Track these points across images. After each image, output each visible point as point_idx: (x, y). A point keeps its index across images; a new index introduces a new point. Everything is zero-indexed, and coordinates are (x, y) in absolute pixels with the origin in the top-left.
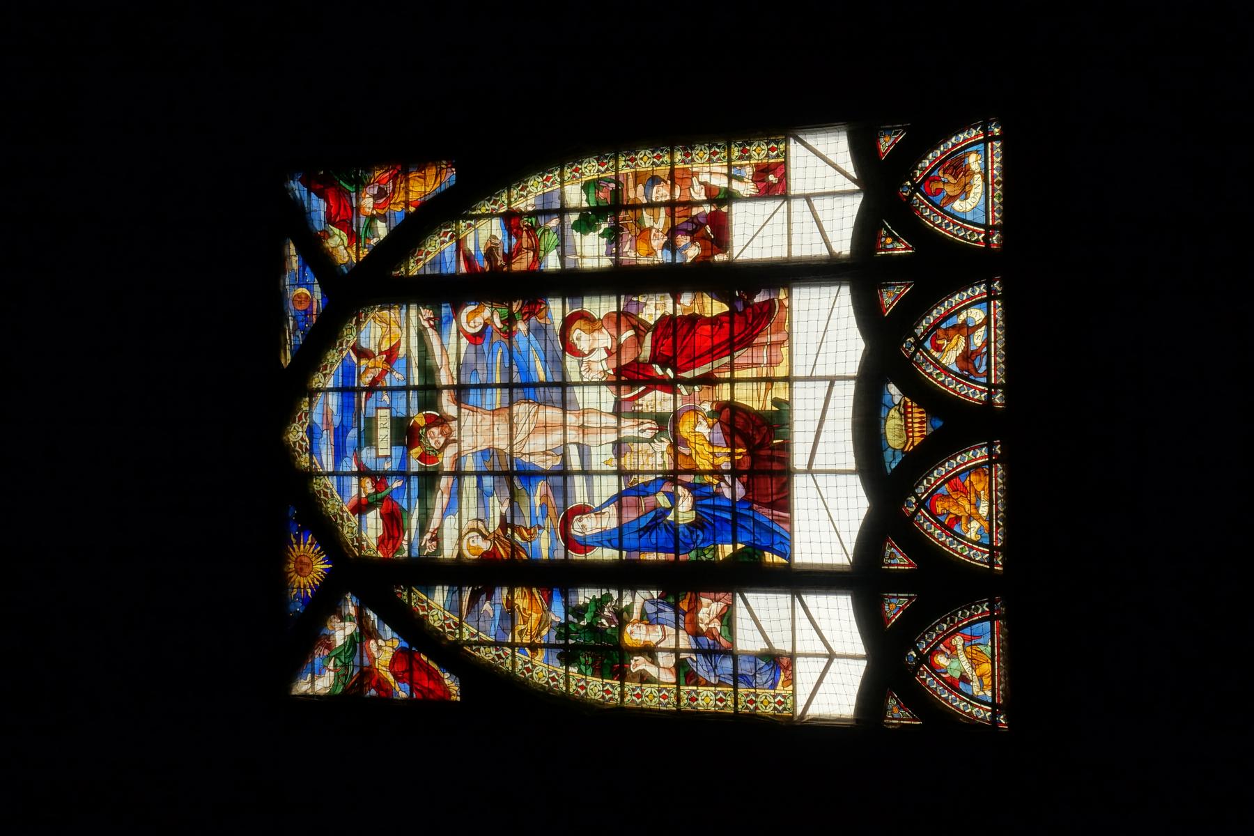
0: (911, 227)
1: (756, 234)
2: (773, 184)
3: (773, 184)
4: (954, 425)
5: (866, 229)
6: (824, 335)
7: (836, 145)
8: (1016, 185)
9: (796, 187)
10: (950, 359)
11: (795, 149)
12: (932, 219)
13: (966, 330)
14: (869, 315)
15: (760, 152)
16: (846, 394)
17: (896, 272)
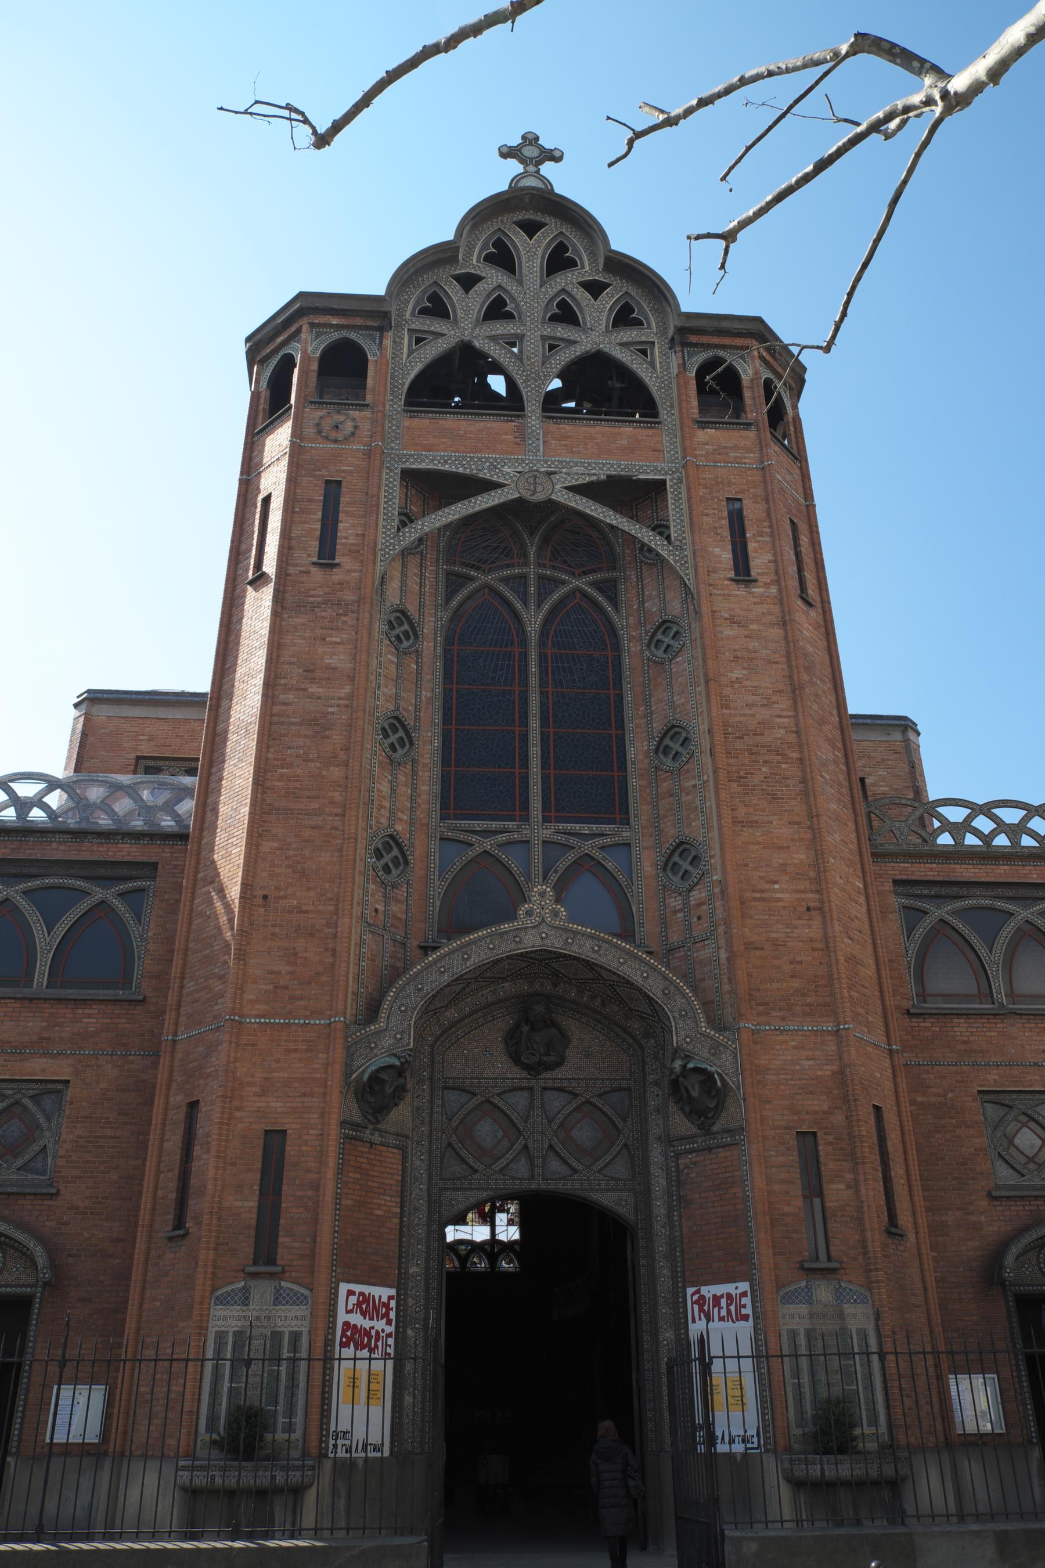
0: (500, 1252)
1: (501, 1218)
2: (510, 1223)
3: (510, 1223)
4: (463, 1260)
5: (501, 1242)
6: (480, 1233)
7: (517, 1236)
8: (507, 1274)
9: (510, 1228)
10: (475, 1260)
11: (516, 1228)
12: (502, 1256)
13: (480, 1263)
14: (484, 1243)
15: (517, 1220)
16: (469, 1237)
17: (493, 1248)
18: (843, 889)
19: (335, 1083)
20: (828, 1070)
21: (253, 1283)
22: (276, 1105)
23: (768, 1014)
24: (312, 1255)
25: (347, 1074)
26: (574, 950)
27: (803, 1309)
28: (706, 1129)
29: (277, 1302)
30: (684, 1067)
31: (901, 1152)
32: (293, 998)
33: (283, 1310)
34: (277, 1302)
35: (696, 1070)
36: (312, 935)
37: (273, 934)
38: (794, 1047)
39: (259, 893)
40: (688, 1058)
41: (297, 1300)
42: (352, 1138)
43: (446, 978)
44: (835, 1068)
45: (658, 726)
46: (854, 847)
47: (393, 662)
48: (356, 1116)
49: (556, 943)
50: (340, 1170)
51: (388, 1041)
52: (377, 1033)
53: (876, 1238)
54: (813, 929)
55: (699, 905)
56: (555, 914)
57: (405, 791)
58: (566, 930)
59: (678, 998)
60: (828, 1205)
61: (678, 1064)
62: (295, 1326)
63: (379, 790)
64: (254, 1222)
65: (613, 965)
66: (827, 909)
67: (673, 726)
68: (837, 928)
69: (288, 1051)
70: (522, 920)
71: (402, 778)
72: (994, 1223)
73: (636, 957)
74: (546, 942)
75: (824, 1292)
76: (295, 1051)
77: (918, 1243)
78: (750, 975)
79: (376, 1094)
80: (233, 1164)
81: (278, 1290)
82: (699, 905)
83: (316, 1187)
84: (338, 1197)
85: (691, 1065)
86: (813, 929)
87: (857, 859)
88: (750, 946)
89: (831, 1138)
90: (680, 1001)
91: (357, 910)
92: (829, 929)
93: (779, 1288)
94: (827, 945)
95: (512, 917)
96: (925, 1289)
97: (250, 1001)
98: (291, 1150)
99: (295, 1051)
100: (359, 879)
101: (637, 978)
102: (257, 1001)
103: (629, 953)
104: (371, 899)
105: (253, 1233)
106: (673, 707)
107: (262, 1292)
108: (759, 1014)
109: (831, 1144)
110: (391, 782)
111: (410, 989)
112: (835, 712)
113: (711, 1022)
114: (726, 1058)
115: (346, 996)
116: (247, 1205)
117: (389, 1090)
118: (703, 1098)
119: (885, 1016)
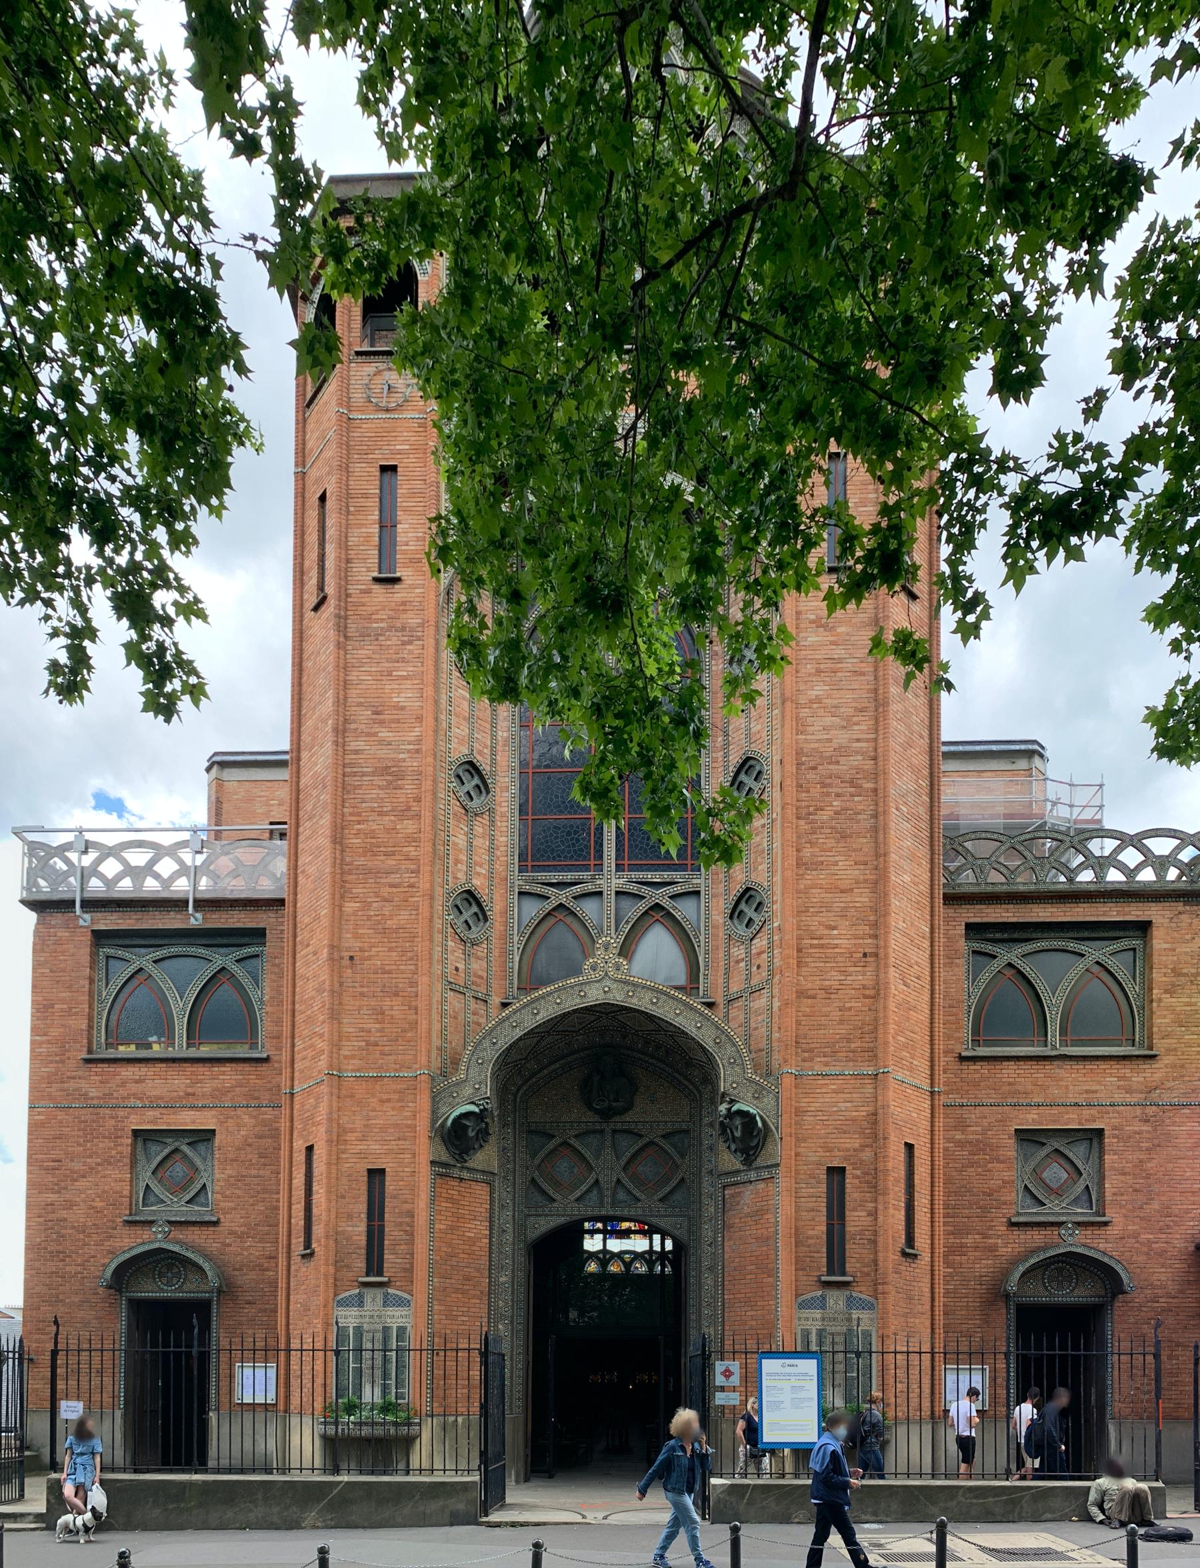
18: (906, 935)
19: (423, 1125)
20: (863, 1112)
21: (365, 1290)
22: (375, 1147)
23: (811, 1060)
24: (411, 1270)
25: (433, 1122)
26: (634, 1003)
27: (817, 1314)
28: (749, 1161)
29: (385, 1304)
30: (729, 1110)
31: (928, 1184)
32: (382, 1054)
33: (390, 1311)
34: (385, 1304)
35: (740, 1113)
36: (396, 994)
37: (362, 994)
38: (834, 1091)
39: (346, 954)
40: (732, 1101)
41: (401, 1303)
42: (441, 1175)
43: (519, 1033)
44: (871, 1109)
45: (735, 759)
46: (925, 888)
47: (464, 698)
48: (445, 1157)
49: (617, 997)
50: (433, 1200)
51: (468, 1091)
52: (457, 1084)
53: (890, 1256)
54: (861, 977)
55: (759, 954)
56: (618, 967)
57: (481, 843)
58: (626, 982)
59: (728, 1046)
60: (848, 1229)
61: (723, 1108)
62: (401, 1322)
63: (456, 844)
64: (364, 1243)
65: (669, 1017)
66: (881, 955)
67: (748, 759)
68: (892, 972)
69: (382, 1101)
70: (588, 973)
71: (479, 830)
72: (1011, 1244)
73: (692, 1008)
74: (610, 996)
75: (836, 1300)
76: (389, 1100)
77: (932, 1261)
78: (798, 1023)
79: (459, 1138)
80: (343, 1197)
81: (386, 1295)
82: (759, 954)
83: (410, 1214)
84: (432, 1223)
85: (734, 1108)
86: (861, 977)
87: (926, 901)
88: (801, 994)
89: (858, 1172)
90: (730, 1050)
91: (437, 969)
92: (882, 976)
93: (797, 1296)
94: (876, 993)
95: (577, 972)
96: (933, 1300)
97: (346, 1057)
98: (390, 1186)
99: (389, 1100)
100: (438, 938)
101: (691, 1029)
102: (353, 1057)
103: (686, 1004)
104: (450, 957)
105: (364, 1251)
106: (748, 735)
107: (373, 1299)
108: (804, 1060)
109: (857, 1177)
110: (466, 834)
111: (486, 1044)
112: (926, 733)
113: (756, 1067)
114: (769, 1101)
115: (429, 1051)
116: (358, 1230)
117: (471, 1134)
118: (750, 1138)
119: (932, 1060)
